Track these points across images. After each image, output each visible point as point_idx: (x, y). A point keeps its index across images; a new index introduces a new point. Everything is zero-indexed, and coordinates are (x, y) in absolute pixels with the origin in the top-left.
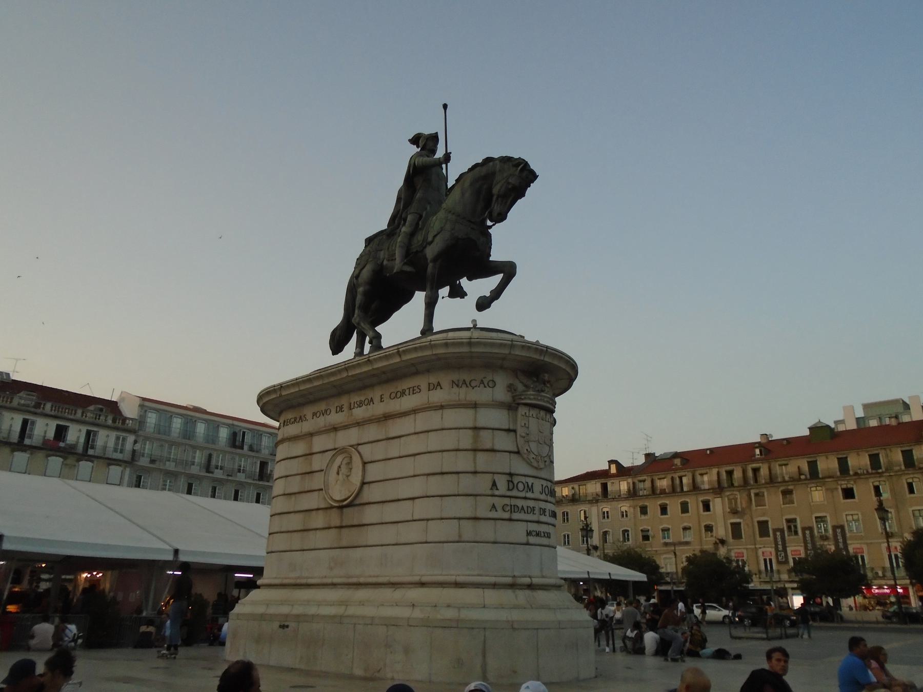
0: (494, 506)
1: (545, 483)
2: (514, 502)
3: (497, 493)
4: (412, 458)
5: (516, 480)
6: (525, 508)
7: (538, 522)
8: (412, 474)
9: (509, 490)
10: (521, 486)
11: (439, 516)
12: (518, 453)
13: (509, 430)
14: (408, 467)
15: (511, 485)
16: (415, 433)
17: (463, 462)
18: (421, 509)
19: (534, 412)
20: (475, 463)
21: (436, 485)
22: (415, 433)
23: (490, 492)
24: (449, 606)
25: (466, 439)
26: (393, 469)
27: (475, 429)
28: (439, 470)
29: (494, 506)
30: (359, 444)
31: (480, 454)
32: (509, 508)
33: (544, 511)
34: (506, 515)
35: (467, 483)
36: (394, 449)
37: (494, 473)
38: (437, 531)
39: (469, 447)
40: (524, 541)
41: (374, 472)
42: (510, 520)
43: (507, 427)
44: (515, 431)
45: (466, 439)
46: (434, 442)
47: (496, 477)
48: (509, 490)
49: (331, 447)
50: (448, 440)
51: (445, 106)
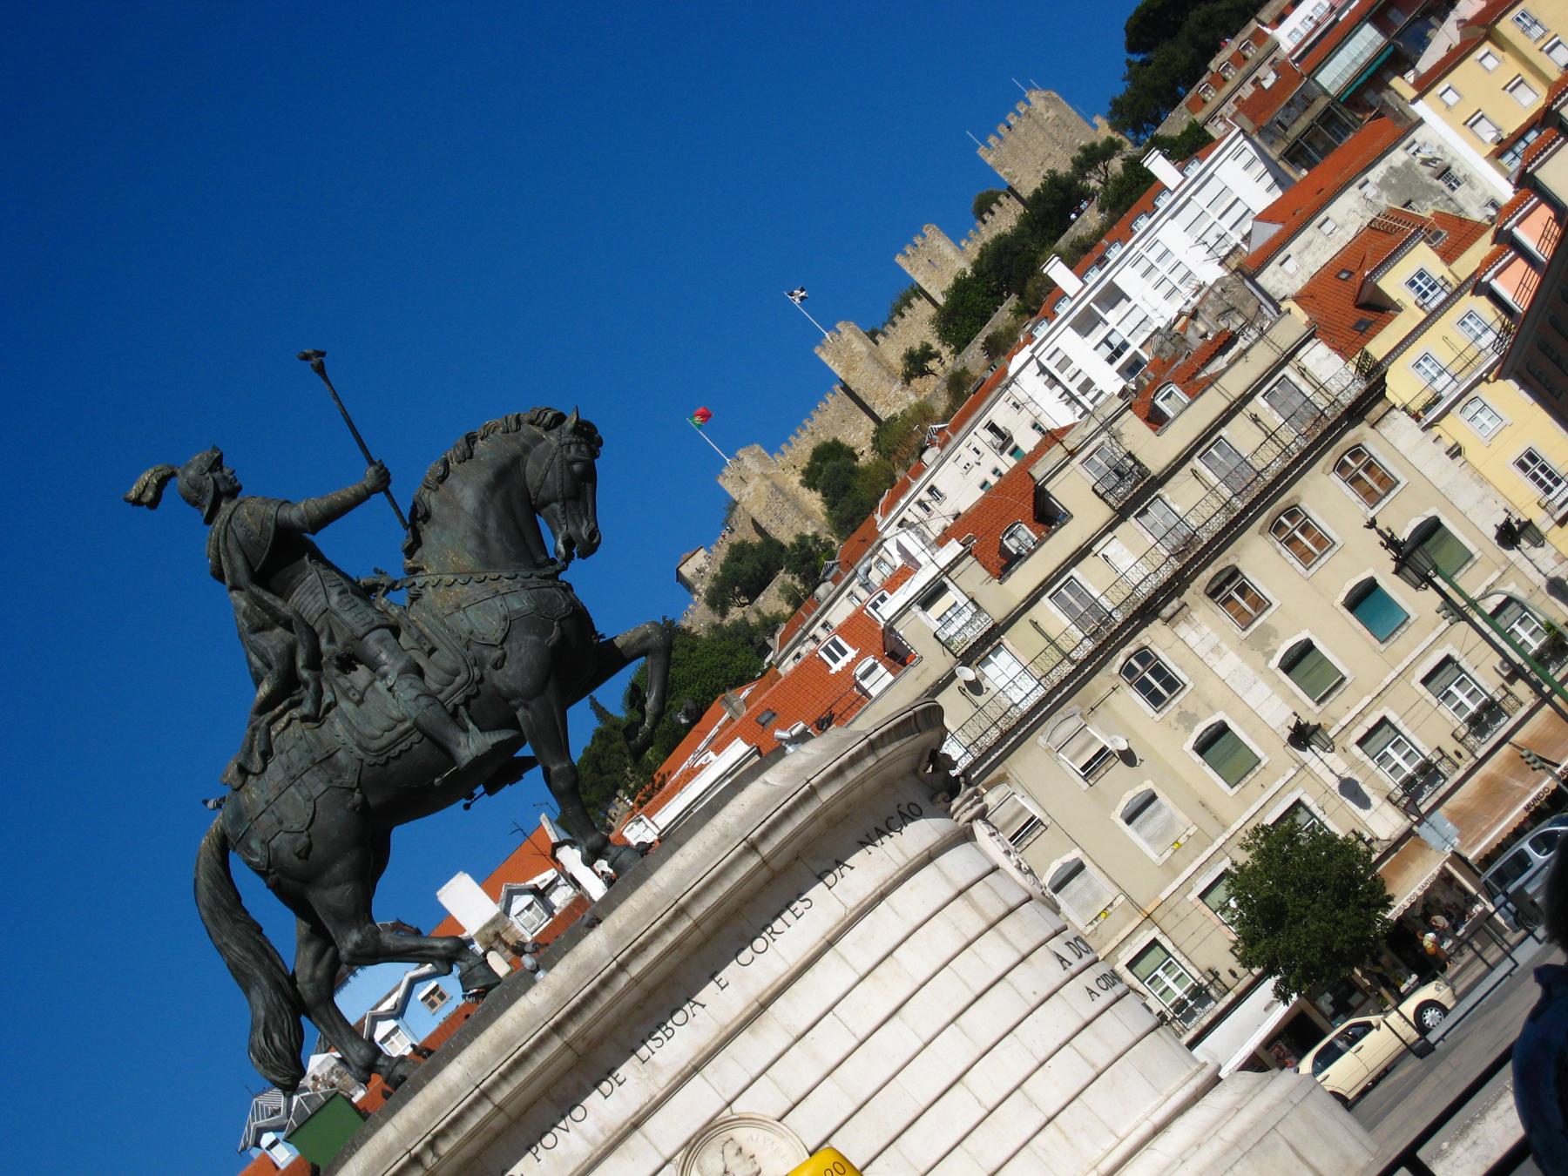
3: (1074, 969)
4: (896, 1019)
8: (920, 1044)
11: (1036, 1063)
14: (898, 1040)
16: (862, 979)
17: (994, 954)
18: (989, 1081)
20: (1011, 944)
22: (862, 979)
23: (1066, 975)
24: (1199, 1146)
27: (960, 893)
28: (971, 997)
29: (1091, 992)
30: (729, 1104)
31: (1003, 925)
36: (830, 1042)
38: (1050, 1089)
39: (983, 925)
42: (1118, 999)
44: (995, 869)
45: (965, 919)
46: (915, 961)
49: (660, 1162)
50: (942, 938)
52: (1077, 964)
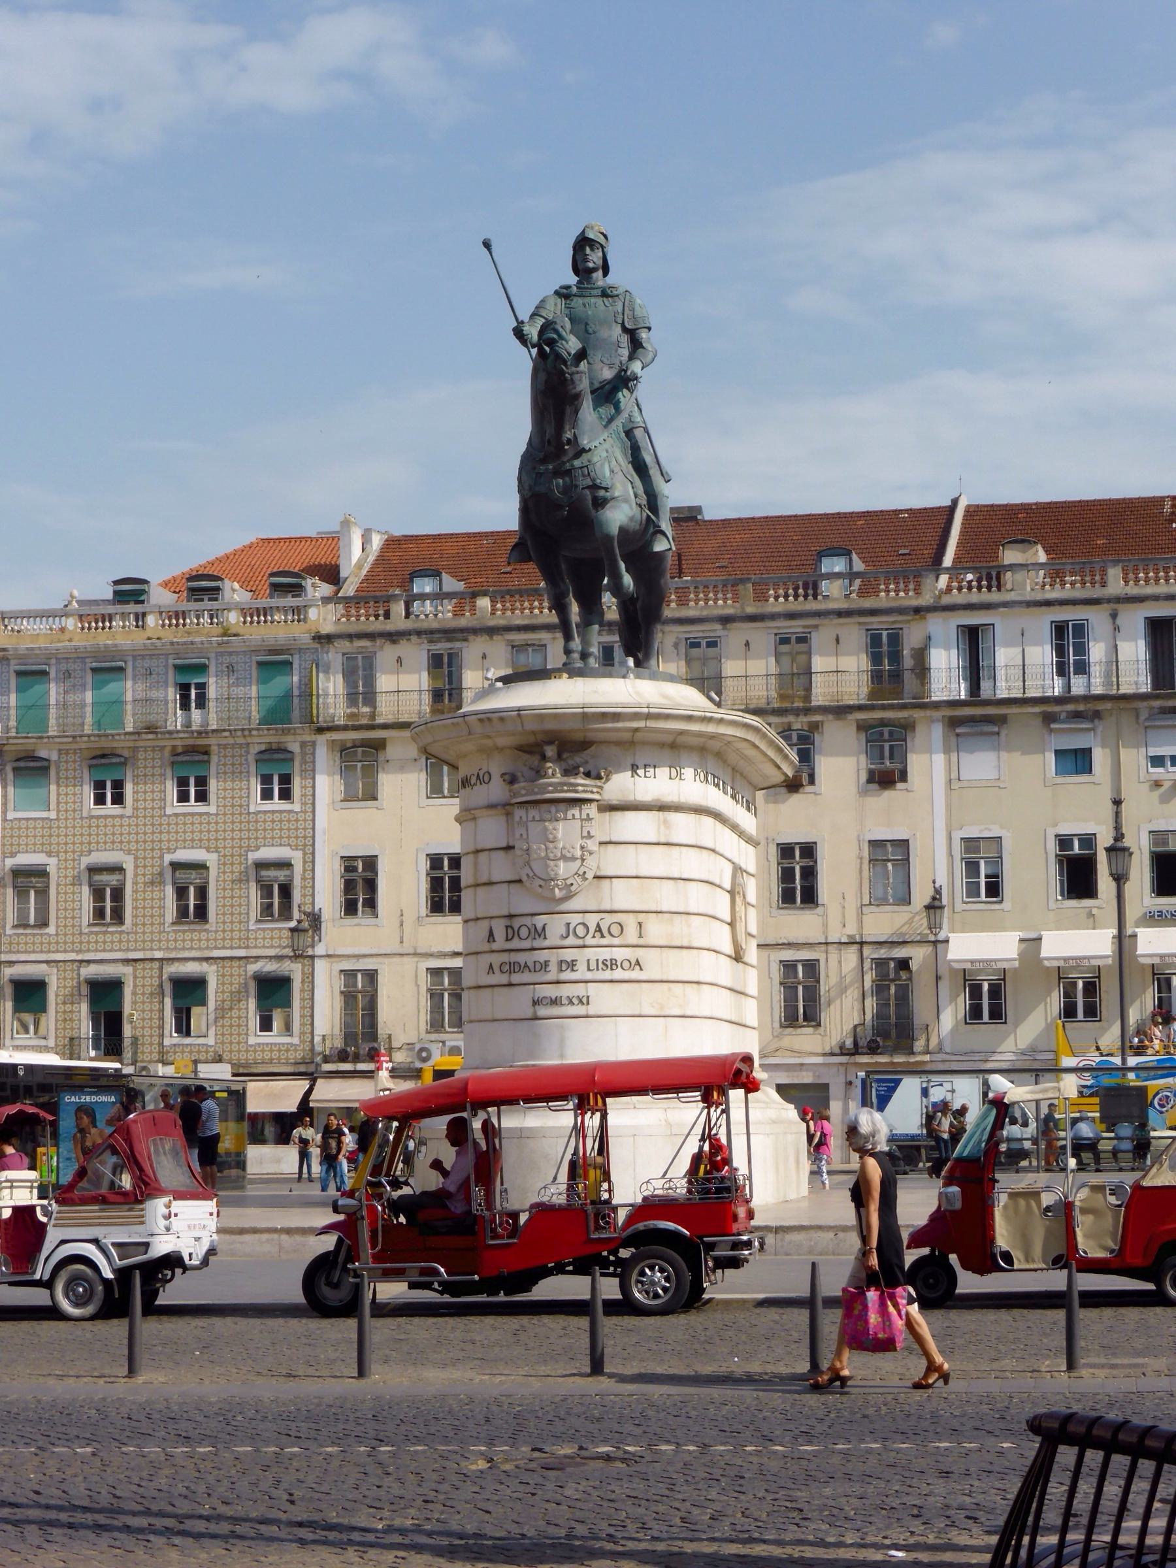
0: (491, 966)
1: (575, 919)
2: (515, 957)
3: (495, 946)
5: (516, 923)
6: (531, 965)
7: (558, 982)
9: (507, 940)
10: (524, 932)
12: (520, 881)
13: (509, 848)
15: (512, 933)
19: (533, 812)
29: (491, 966)
31: (480, 890)
32: (507, 967)
33: (572, 965)
34: (504, 979)
37: (491, 918)
40: (529, 1014)
42: (510, 985)
43: (504, 845)
47: (494, 923)
48: (507, 940)
51: (487, 245)
52: (500, 943)
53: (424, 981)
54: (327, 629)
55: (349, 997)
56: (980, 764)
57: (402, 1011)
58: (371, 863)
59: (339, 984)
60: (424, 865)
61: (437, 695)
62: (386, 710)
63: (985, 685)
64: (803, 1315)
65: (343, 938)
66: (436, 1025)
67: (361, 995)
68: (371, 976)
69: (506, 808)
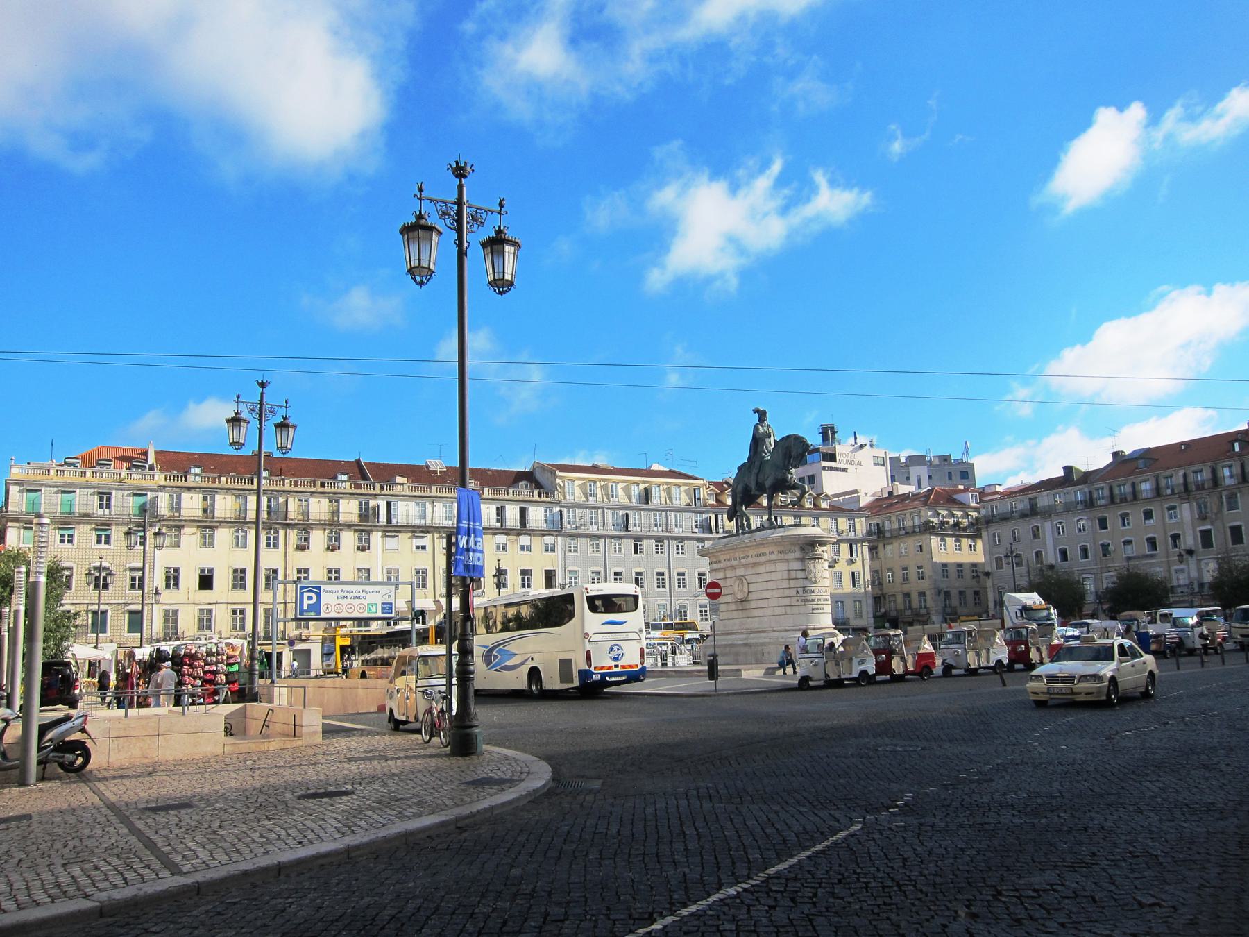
21: (776, 594)
25: (785, 575)
26: (759, 586)
35: (787, 592)
36: (759, 578)
38: (778, 611)
41: (752, 587)
45: (786, 576)
50: (779, 576)
53: (197, 612)
54: (163, 483)
55: (166, 621)
56: (392, 542)
57: (188, 623)
58: (177, 570)
59: (162, 614)
60: (198, 572)
61: (205, 511)
62: (185, 513)
63: (394, 521)
64: (1226, 655)
65: (169, 598)
66: (201, 628)
67: (171, 618)
68: (176, 612)
69: (802, 560)
